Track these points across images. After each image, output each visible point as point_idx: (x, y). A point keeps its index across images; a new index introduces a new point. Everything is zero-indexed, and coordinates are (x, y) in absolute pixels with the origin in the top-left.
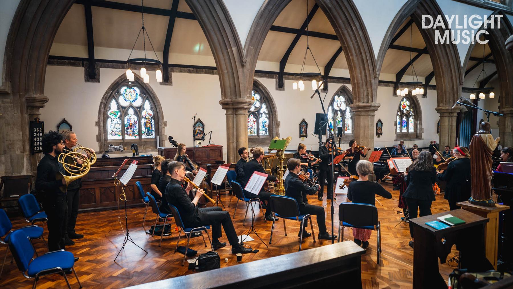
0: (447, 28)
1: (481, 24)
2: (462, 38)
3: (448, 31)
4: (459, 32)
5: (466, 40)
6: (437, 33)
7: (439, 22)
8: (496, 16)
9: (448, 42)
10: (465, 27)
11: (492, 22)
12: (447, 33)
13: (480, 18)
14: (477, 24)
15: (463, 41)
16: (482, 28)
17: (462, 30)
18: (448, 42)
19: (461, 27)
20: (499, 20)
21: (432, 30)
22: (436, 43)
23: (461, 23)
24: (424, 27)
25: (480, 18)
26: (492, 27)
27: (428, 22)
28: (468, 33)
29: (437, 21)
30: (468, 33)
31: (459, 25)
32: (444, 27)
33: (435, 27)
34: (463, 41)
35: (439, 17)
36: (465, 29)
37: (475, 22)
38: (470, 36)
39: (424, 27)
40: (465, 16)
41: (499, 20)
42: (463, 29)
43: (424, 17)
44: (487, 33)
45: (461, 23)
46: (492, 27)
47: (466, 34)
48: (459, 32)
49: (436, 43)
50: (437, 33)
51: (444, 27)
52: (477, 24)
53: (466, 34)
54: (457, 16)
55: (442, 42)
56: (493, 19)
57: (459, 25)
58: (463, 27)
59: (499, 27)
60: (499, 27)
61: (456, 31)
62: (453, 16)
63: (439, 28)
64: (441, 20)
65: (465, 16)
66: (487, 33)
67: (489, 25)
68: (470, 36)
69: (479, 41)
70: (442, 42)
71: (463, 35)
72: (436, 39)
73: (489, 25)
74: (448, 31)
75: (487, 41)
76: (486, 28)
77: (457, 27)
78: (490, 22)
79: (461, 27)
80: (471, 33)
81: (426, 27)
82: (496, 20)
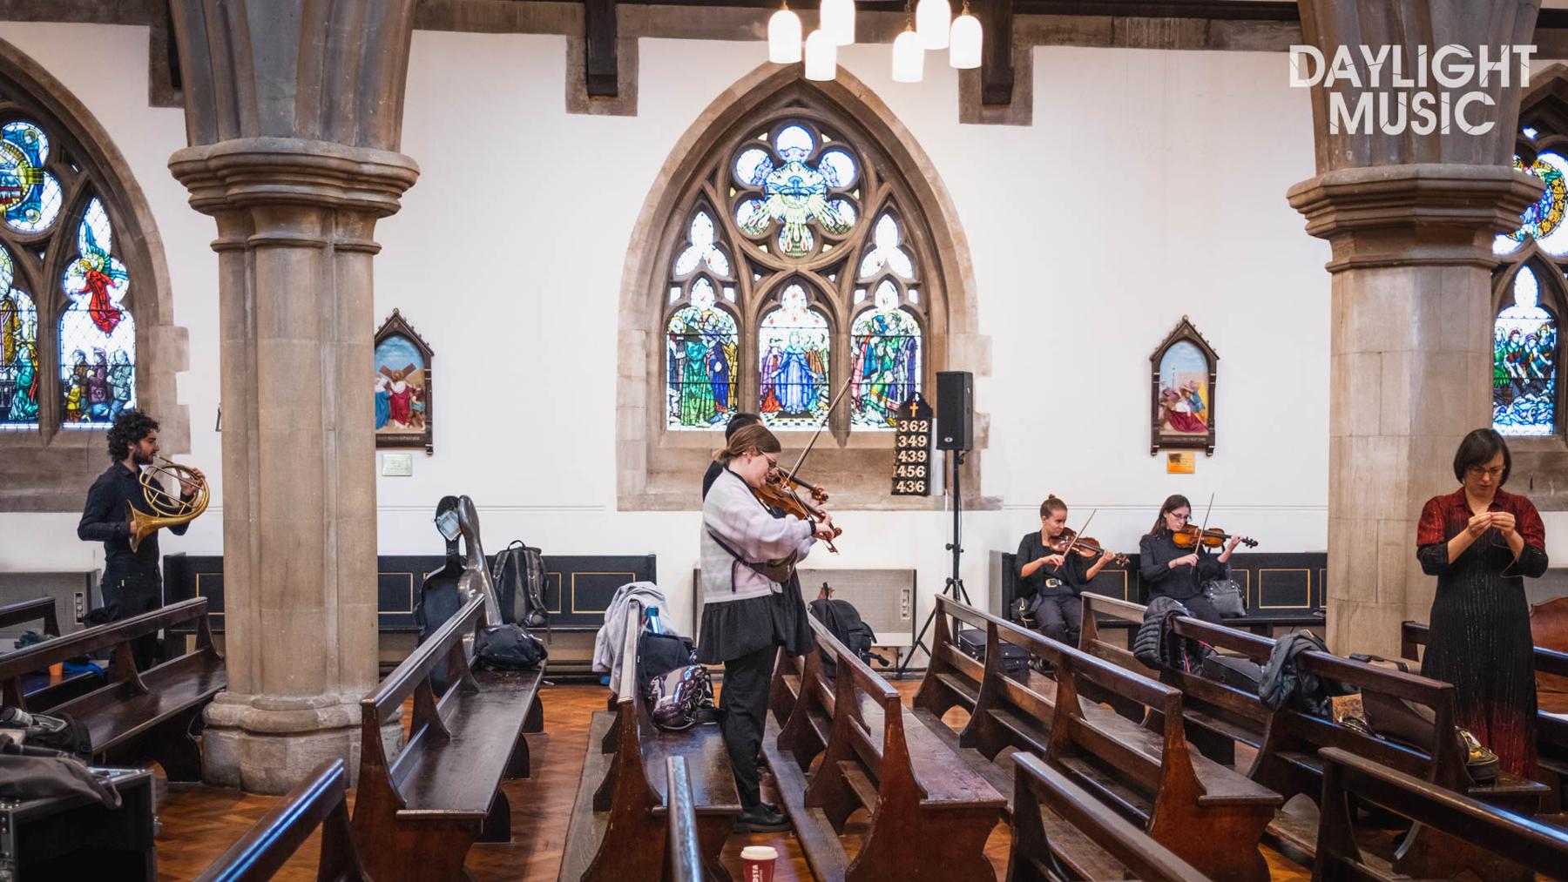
0: (1367, 87)
1: (1469, 70)
2: (1412, 115)
3: (1371, 95)
4: (1402, 97)
5: (1424, 122)
7: (1343, 67)
8: (1517, 49)
9: (1369, 130)
10: (1423, 83)
11: (1504, 66)
12: (1366, 99)
13: (1466, 54)
14: (1458, 75)
15: (1415, 125)
16: (1474, 85)
17: (1411, 93)
18: (1369, 130)
19: (1410, 83)
20: (1525, 59)
23: (1409, 70)
25: (1469, 55)
26: (1505, 82)
28: (1431, 100)
29: (1336, 64)
30: (1431, 100)
31: (1405, 76)
32: (1357, 83)
33: (1329, 83)
34: (1415, 125)
35: (1343, 52)
36: (1423, 89)
37: (1452, 68)
38: (1436, 109)
40: (1422, 49)
42: (1417, 89)
44: (1489, 101)
45: (1409, 70)
46: (1505, 82)
47: (1424, 103)
49: (1334, 130)
51: (1357, 83)
52: (1459, 75)
53: (1424, 103)
54: (1397, 49)
55: (1351, 128)
56: (1505, 56)
57: (1405, 76)
58: (1416, 83)
62: (1385, 49)
63: (1342, 85)
64: (1349, 60)
65: (1422, 49)
66: (1489, 101)
67: (1494, 76)
69: (1464, 125)
70: (1351, 128)
71: (1416, 106)
72: (1334, 119)
73: (1494, 76)
74: (1371, 95)
75: (1487, 127)
76: (1484, 83)
77: (1398, 82)
78: (1497, 66)
79: (1410, 83)
80: (1438, 99)
82: (1515, 60)
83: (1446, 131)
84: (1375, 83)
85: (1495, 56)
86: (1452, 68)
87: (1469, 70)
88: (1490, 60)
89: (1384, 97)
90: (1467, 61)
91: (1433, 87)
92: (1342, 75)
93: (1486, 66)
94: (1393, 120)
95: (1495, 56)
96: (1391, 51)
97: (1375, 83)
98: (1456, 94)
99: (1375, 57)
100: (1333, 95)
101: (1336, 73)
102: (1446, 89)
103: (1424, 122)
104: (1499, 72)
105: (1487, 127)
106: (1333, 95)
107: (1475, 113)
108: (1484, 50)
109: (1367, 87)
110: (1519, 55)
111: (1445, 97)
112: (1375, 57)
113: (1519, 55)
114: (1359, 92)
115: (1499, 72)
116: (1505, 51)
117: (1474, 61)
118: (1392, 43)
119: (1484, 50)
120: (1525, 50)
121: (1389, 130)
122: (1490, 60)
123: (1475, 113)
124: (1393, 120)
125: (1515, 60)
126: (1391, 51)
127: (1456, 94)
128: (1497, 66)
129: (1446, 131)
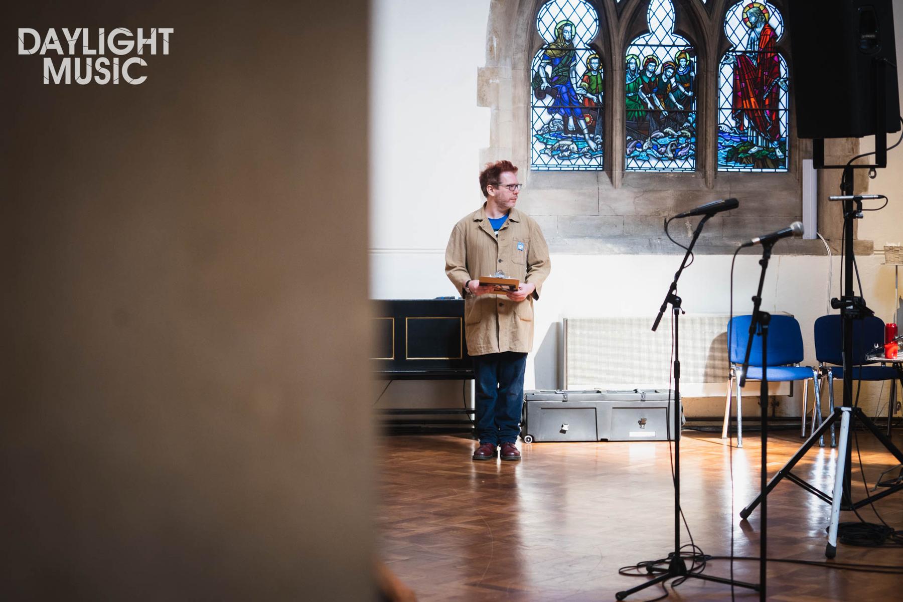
0: (66, 54)
1: (130, 44)
2: (95, 72)
4: (89, 61)
5: (102, 76)
6: (48, 63)
7: (52, 42)
8: (161, 30)
9: (68, 81)
10: (102, 52)
11: (153, 41)
12: (66, 62)
13: (129, 33)
14: (124, 47)
15: (97, 78)
16: (134, 53)
17: (95, 58)
18: (68, 81)
19: (94, 52)
20: (166, 38)
21: (38, 59)
22: (46, 82)
23: (94, 44)
24: (22, 51)
25: (129, 33)
26: (154, 51)
27: (29, 42)
28: (107, 62)
29: (47, 40)
30: (107, 62)
31: (90, 48)
32: (60, 52)
33: (43, 52)
34: (97, 78)
35: (52, 33)
36: (102, 56)
37: (120, 43)
39: (22, 51)
40: (102, 31)
41: (166, 38)
43: (22, 32)
44: (143, 63)
45: (94, 44)
46: (154, 51)
47: (102, 65)
49: (46, 82)
50: (48, 63)
51: (60, 52)
52: (124, 47)
53: (102, 65)
54: (86, 31)
55: (57, 80)
57: (90, 48)
58: (98, 52)
59: (166, 51)
60: (166, 51)
61: (83, 59)
62: (78, 31)
63: (51, 53)
64: (55, 38)
65: (102, 31)
66: (143, 63)
67: (147, 47)
70: (57, 80)
71: (98, 67)
73: (147, 47)
75: (142, 79)
76: (141, 52)
77: (86, 51)
78: (149, 42)
79: (94, 52)
81: (26, 52)
82: (160, 37)
83: (116, 82)
84: (72, 51)
85: (147, 35)
86: (120, 43)
87: (130, 44)
88: (144, 37)
89: (77, 61)
90: (129, 38)
91: (109, 54)
92: (51, 47)
93: (141, 41)
94: (83, 75)
95: (147, 35)
96: (82, 33)
97: (72, 51)
98: (123, 59)
99: (72, 36)
100: (45, 59)
101: (47, 46)
102: (116, 56)
103: (102, 76)
104: (150, 45)
105: (142, 79)
106: (45, 59)
107: (135, 71)
108: (140, 31)
109: (66, 54)
110: (162, 34)
112: (72, 36)
113: (162, 34)
114: (61, 57)
115: (150, 45)
116: (153, 32)
117: (134, 38)
118: (83, 27)
119: (140, 31)
120: (166, 32)
121: (81, 81)
122: (144, 37)
123: (135, 71)
124: (83, 75)
125: (160, 37)
126: (82, 33)
127: (123, 59)
128: (149, 42)
129: (116, 82)
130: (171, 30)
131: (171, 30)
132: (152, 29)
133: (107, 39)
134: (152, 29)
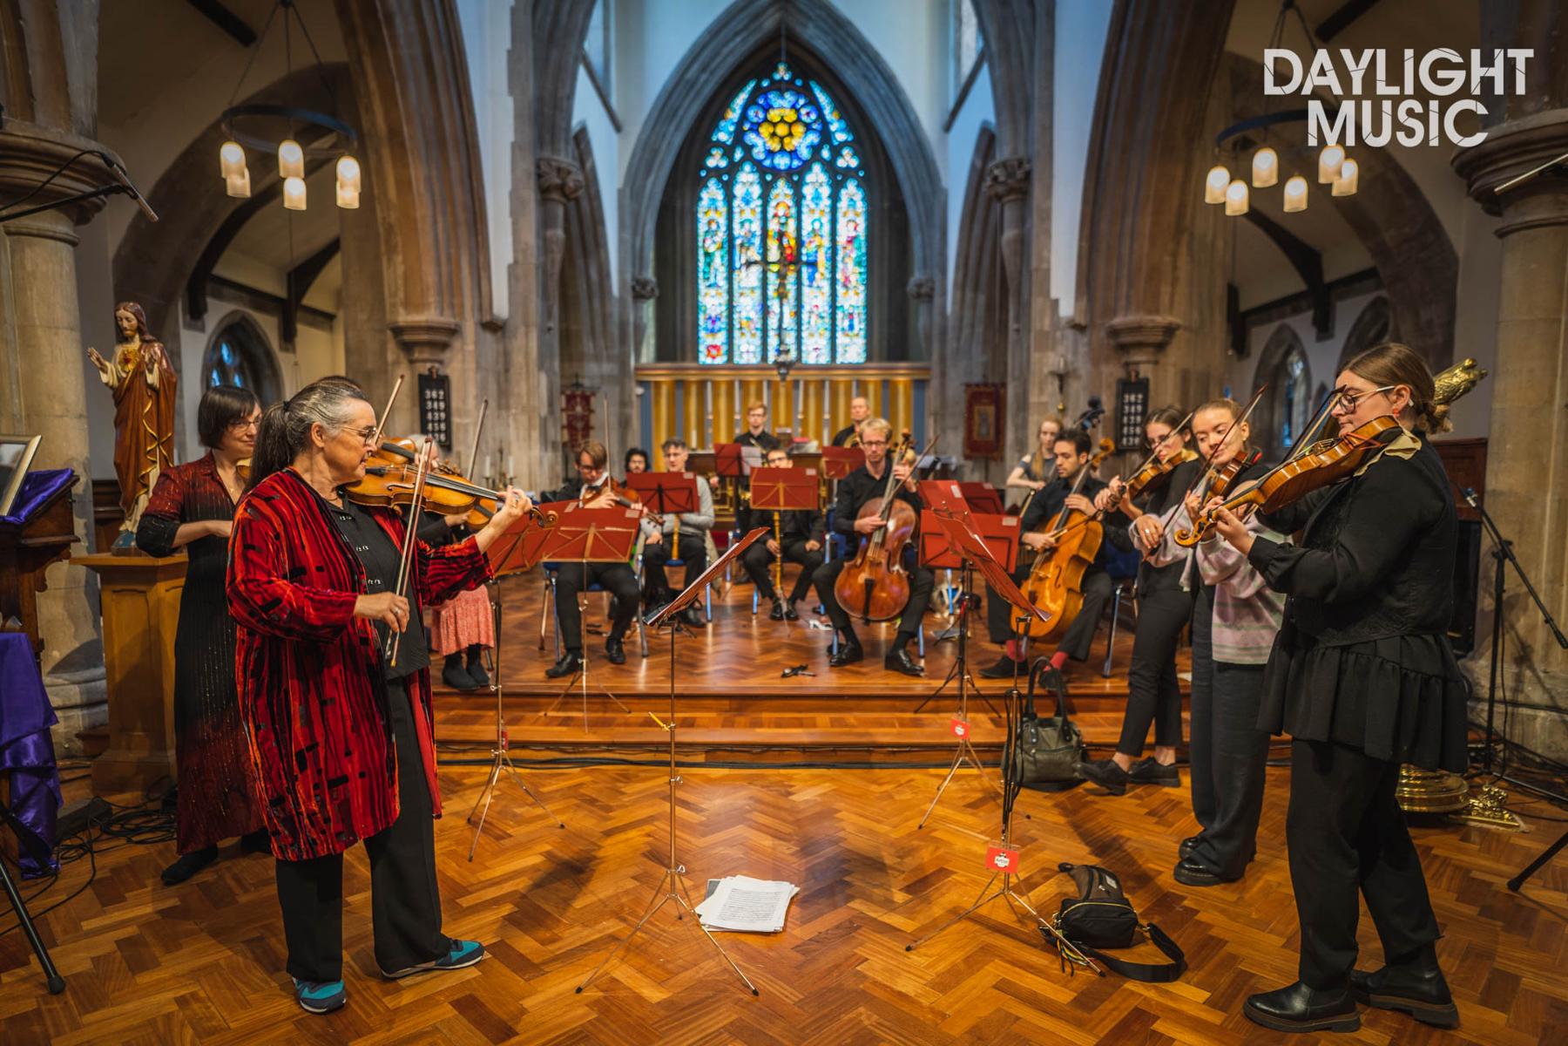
1: (1459, 77)
2: (1397, 126)
4: (1387, 106)
5: (1410, 133)
8: (1512, 53)
10: (1409, 90)
11: (1497, 72)
13: (1456, 58)
15: (1401, 136)
16: (1464, 92)
17: (1396, 101)
19: (1395, 90)
20: (1521, 65)
23: (1395, 76)
25: (1456, 58)
26: (1499, 89)
28: (1418, 108)
30: (1418, 108)
34: (1401, 136)
36: (1409, 97)
37: (1442, 74)
38: (1424, 118)
40: (1409, 53)
41: (1521, 65)
44: (1482, 110)
45: (1395, 76)
46: (1499, 89)
47: (1410, 113)
48: (1387, 106)
53: (1410, 113)
57: (1389, 83)
58: (1402, 90)
59: (1521, 89)
60: (1521, 89)
61: (1377, 102)
65: (1409, 53)
66: (1482, 110)
67: (1487, 83)
68: (1424, 118)
69: (1454, 136)
71: (1402, 116)
73: (1487, 83)
76: (1477, 92)
77: (1382, 89)
78: (1491, 72)
79: (1395, 90)
82: (1510, 65)
85: (1487, 61)
86: (1442, 74)
87: (1459, 77)
89: (1367, 105)
91: (1422, 95)
93: (1478, 72)
94: (1377, 131)
95: (1487, 61)
98: (1446, 102)
102: (1435, 97)
103: (1410, 133)
104: (1492, 79)
107: (1466, 123)
108: (1476, 54)
111: (1434, 105)
115: (1492, 79)
116: (1499, 55)
117: (1466, 66)
119: (1476, 54)
120: (1521, 55)
123: (1466, 123)
124: (1377, 131)
125: (1510, 65)
127: (1446, 102)
128: (1491, 72)
130: (1530, 53)
131: (1530, 53)
132: (1497, 51)
133: (1418, 68)
134: (1497, 51)
